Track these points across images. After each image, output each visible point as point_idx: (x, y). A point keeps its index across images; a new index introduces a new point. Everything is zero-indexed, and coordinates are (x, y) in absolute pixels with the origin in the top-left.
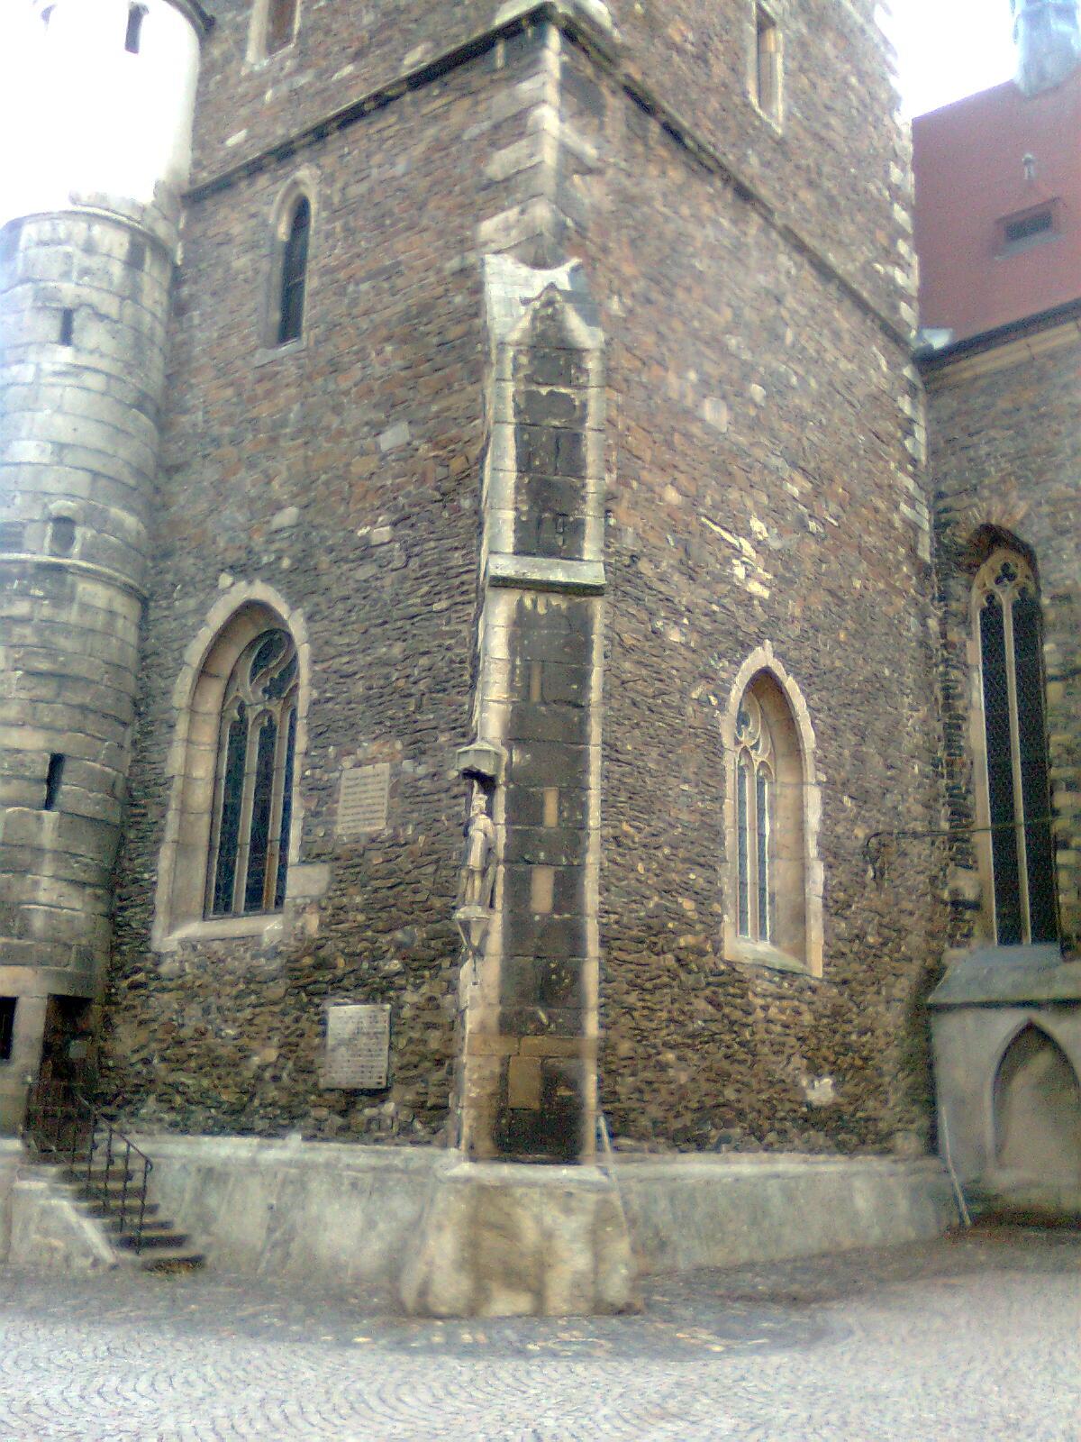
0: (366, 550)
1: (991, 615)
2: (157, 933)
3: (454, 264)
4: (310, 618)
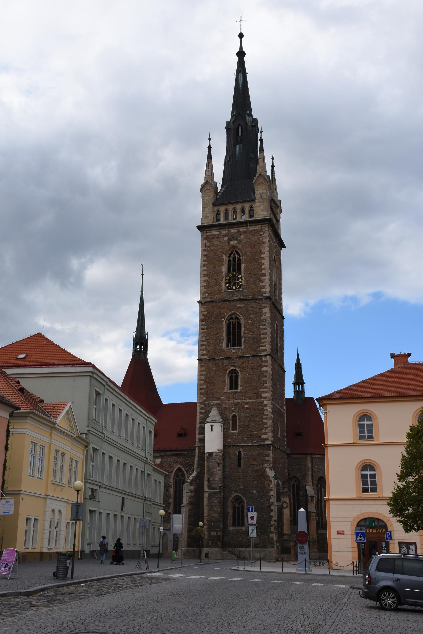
0: (253, 493)
1: (294, 485)
2: (229, 528)
3: (262, 467)
4: (246, 499)
